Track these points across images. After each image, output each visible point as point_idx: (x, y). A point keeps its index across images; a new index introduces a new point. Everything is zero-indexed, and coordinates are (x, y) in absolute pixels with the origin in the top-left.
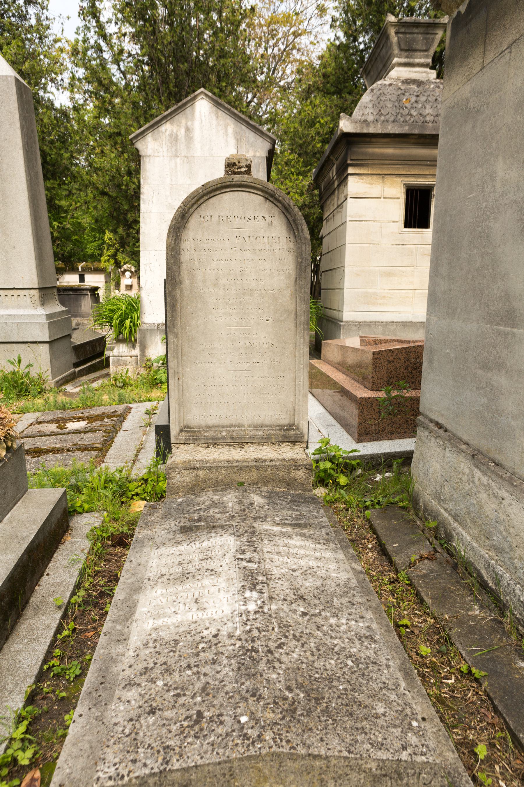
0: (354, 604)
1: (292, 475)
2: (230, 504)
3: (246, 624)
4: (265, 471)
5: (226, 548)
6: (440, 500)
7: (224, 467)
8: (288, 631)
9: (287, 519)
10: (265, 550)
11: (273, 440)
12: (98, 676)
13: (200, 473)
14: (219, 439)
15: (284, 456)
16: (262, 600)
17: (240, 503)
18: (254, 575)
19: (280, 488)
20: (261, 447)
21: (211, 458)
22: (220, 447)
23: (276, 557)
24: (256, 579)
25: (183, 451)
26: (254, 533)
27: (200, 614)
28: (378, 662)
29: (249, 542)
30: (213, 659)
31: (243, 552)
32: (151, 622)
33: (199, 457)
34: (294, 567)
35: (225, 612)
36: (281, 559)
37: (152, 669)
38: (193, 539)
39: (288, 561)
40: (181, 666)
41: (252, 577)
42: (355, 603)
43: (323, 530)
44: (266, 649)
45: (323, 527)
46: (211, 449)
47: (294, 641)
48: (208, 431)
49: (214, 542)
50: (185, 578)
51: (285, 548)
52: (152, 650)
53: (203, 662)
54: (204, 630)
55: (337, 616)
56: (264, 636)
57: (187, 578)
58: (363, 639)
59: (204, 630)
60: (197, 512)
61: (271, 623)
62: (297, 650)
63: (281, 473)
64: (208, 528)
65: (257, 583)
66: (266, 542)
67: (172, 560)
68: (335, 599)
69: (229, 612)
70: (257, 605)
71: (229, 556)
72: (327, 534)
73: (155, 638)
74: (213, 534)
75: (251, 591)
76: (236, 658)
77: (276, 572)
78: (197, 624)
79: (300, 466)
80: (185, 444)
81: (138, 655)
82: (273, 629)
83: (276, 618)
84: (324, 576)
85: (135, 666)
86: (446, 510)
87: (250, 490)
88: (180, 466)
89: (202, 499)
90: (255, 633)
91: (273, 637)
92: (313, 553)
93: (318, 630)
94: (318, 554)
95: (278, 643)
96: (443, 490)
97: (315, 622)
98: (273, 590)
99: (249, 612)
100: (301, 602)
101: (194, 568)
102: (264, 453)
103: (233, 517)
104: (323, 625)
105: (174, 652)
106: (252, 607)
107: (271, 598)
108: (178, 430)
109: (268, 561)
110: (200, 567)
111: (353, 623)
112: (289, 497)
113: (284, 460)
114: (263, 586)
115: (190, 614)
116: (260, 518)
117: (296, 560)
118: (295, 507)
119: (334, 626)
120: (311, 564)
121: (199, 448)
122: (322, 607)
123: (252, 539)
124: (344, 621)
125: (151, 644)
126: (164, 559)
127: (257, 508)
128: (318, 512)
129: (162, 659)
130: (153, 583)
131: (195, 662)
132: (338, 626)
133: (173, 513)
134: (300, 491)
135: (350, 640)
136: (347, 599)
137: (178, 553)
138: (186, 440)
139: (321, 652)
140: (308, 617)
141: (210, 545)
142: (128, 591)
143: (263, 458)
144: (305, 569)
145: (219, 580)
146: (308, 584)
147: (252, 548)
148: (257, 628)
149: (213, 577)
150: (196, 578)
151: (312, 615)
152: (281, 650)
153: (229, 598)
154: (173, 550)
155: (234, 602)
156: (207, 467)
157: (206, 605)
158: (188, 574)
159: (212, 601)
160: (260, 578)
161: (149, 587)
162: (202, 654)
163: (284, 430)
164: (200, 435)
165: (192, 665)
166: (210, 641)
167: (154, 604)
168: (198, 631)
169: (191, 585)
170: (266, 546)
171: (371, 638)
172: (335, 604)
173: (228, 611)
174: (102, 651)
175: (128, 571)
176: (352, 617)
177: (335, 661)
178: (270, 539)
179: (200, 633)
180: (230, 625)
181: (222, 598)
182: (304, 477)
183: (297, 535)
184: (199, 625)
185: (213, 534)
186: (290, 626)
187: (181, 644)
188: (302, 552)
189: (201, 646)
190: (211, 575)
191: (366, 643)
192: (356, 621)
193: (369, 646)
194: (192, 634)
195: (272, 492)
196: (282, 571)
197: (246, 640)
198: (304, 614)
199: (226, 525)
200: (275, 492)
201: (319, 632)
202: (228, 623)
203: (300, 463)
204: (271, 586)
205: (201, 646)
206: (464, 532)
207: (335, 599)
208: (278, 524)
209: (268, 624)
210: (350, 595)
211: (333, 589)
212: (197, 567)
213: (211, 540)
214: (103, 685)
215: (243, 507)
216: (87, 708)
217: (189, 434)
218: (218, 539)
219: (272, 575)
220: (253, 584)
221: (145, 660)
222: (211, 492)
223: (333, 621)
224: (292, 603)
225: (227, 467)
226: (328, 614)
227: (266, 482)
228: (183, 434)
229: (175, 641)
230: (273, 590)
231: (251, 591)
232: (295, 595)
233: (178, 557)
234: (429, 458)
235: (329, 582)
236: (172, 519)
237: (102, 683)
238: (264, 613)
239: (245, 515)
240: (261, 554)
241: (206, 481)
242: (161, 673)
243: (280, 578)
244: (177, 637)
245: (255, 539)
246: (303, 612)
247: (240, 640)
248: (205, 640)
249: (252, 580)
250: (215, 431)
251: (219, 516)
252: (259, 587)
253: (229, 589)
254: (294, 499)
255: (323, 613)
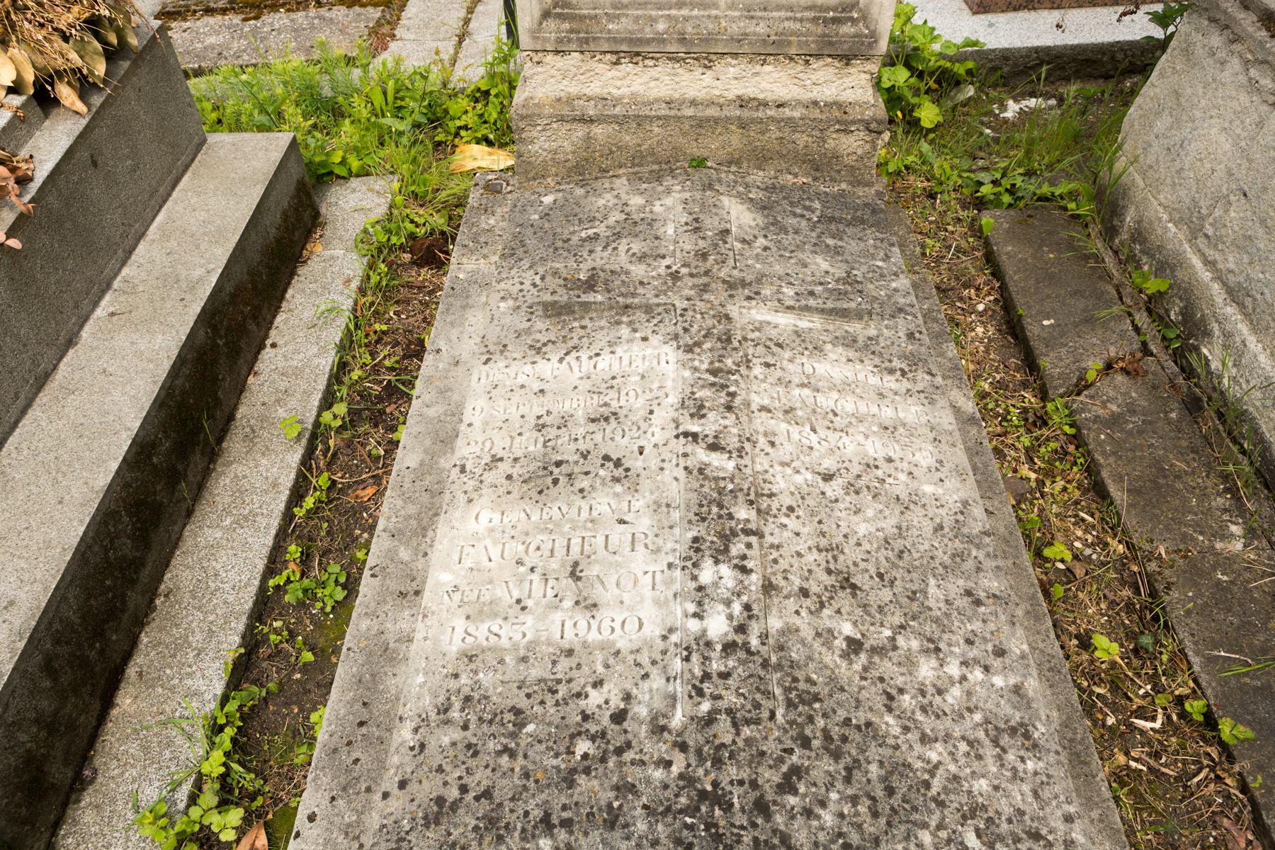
0: (978, 603)
1: (831, 144)
2: (670, 231)
3: (700, 693)
4: (763, 133)
5: (655, 386)
6: (1195, 232)
7: (659, 118)
8: (811, 719)
9: (812, 293)
10: (756, 401)
11: (793, 51)
12: (354, 700)
13: (598, 130)
14: (649, 42)
15: (815, 94)
16: (745, 598)
17: (697, 230)
18: (727, 500)
19: (796, 176)
20: (758, 68)
21: (625, 91)
22: (647, 62)
23: (784, 426)
24: (730, 516)
25: (553, 72)
26: (729, 340)
27: (582, 619)
28: (1044, 832)
29: (714, 372)
30: (610, 805)
31: (699, 412)
32: (460, 624)
33: (595, 89)
34: (829, 464)
35: (647, 630)
36: (795, 431)
37: (455, 806)
38: (575, 341)
39: (814, 437)
40: (526, 814)
41: (721, 506)
42: (983, 595)
43: (900, 321)
44: (753, 796)
45: (901, 310)
46: (626, 67)
47: (826, 758)
48: (618, 17)
49: (625, 362)
50: (549, 480)
51: (806, 392)
52: (456, 734)
53: (584, 811)
54: (589, 689)
55: (938, 650)
56: (748, 741)
57: (555, 482)
58: (1005, 740)
59: (589, 689)
60: (588, 246)
61: (768, 694)
62: (834, 796)
63: (802, 139)
64: (611, 308)
65: (734, 533)
66: (758, 370)
67: (522, 410)
68: (932, 582)
69: (658, 633)
70: (730, 617)
71: (663, 415)
72: (911, 336)
73: (466, 691)
74: (625, 331)
75: (717, 562)
76: (669, 819)
77: (782, 485)
78: (573, 662)
79: (853, 122)
80: (557, 52)
81: (422, 746)
82: (772, 716)
83: (779, 667)
84: (904, 496)
85: (413, 787)
86: (1210, 263)
87: (719, 181)
88: (547, 111)
89: (601, 202)
90: (724, 731)
91: (771, 747)
92: (874, 410)
93: (890, 710)
94: (888, 413)
95: (784, 769)
96: (1217, 213)
97: (882, 679)
98: (775, 554)
99: (708, 644)
100: (844, 600)
101: (573, 447)
102: (764, 85)
103: (675, 276)
104: (901, 691)
105: (513, 755)
106: (718, 626)
107: (768, 588)
108: (537, 14)
109: (762, 441)
110: (590, 446)
111: (977, 675)
112: (817, 205)
113: (815, 103)
114: (749, 546)
115: (558, 616)
116: (744, 284)
117: (833, 437)
118: (830, 242)
119: (931, 690)
120: (871, 452)
121: (593, 64)
122: (897, 619)
123: (722, 359)
124: (954, 669)
125: (455, 714)
126: (502, 403)
127: (738, 245)
128: (887, 258)
129: (482, 778)
130: (471, 484)
131: (564, 808)
132: (940, 692)
133: (531, 242)
134: (844, 186)
135: (970, 743)
136: (961, 582)
137: (536, 386)
138: (560, 41)
139: (896, 801)
140: (863, 657)
141: (616, 369)
142: (428, 442)
143: (761, 96)
144: (856, 469)
145: (637, 505)
146: (862, 529)
147: (723, 399)
148: (729, 712)
149: (618, 488)
150: (578, 485)
151: (874, 650)
152: (792, 800)
153: (658, 576)
154: (524, 372)
155: (670, 594)
156: (615, 116)
157: (597, 593)
158: (558, 464)
159: (613, 579)
160: (743, 513)
161: (462, 498)
162: (581, 780)
163: (825, 21)
164: (595, 29)
165: (555, 820)
166: (603, 734)
167: (468, 563)
168: (576, 687)
169: (564, 509)
170: (758, 389)
171: (1022, 731)
172: (931, 603)
173: (653, 630)
174: (365, 624)
175: (429, 380)
176: (973, 653)
177: (934, 835)
178: (770, 360)
179: (578, 695)
180: (657, 682)
181: (640, 575)
182: (860, 152)
183: (836, 341)
184: (579, 666)
185: (625, 331)
186: (817, 698)
187: (530, 728)
188: (848, 405)
189: (583, 746)
190: (616, 480)
191: (1011, 757)
192: (987, 669)
193: (1020, 767)
194: (559, 696)
195: (774, 187)
196: (799, 479)
197: (699, 752)
198: (854, 646)
199: (658, 305)
200: (782, 188)
201: (889, 719)
202: (654, 672)
203: (855, 114)
204: (769, 539)
205: (583, 746)
206: (1252, 341)
207: (932, 582)
208: (788, 308)
209: (758, 696)
210: (969, 565)
211: (927, 547)
212: (582, 446)
213: (619, 350)
214: (364, 730)
215: (702, 243)
216: (327, 796)
217: (567, 26)
218: (637, 347)
219: (771, 495)
220: (722, 536)
221: (440, 769)
222: (624, 180)
223: (926, 670)
224: (822, 605)
225: (666, 118)
226: (915, 644)
227: (761, 159)
228: (551, 24)
229: (517, 712)
230: (775, 554)
231: (717, 562)
232: (829, 572)
233: (535, 400)
234: (1198, 114)
235: (916, 516)
236: (526, 264)
237: (361, 724)
238: (749, 652)
239: (707, 273)
240: (744, 419)
241: (611, 152)
242: (476, 828)
243: (791, 509)
244: (523, 703)
245: (729, 362)
246: (849, 640)
247: (683, 747)
248: (593, 728)
249: (720, 522)
250: (637, 18)
251: (638, 270)
252: (737, 548)
253: (660, 541)
254: (829, 212)
255: (901, 641)
